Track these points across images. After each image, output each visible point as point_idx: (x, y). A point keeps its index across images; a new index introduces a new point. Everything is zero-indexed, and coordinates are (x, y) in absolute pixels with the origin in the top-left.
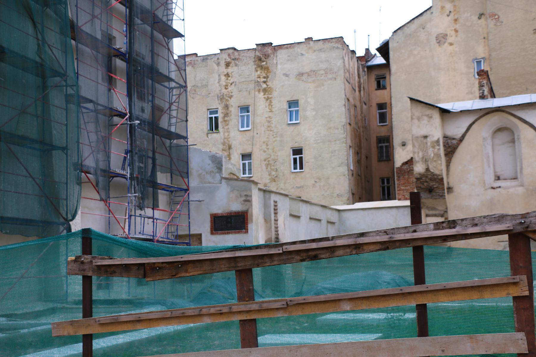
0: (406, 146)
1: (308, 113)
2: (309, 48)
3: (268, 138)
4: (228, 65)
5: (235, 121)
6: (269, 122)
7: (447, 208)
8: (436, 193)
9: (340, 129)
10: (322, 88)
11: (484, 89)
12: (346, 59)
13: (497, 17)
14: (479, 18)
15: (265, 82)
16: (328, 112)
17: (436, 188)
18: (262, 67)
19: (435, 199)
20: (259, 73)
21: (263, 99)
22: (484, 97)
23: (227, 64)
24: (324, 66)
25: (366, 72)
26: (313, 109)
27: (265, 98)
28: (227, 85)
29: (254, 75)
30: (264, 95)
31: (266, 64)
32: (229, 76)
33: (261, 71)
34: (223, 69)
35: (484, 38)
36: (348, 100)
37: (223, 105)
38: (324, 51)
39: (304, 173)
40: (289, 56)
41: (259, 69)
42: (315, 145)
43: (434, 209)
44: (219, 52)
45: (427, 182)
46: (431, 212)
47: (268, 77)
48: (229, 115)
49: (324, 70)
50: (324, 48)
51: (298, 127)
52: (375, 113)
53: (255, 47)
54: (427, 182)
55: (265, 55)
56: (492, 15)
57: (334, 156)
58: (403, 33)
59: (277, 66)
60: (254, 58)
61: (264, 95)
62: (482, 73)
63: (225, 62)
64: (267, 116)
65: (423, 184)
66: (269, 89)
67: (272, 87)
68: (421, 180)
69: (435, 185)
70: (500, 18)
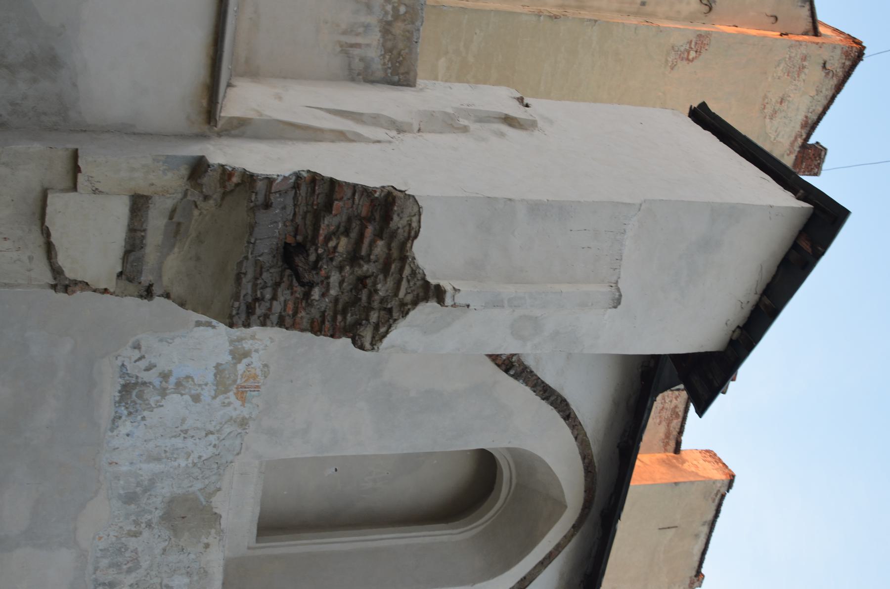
8: (277, 285)
13: (693, 54)
17: (307, 295)
45: (354, 258)
68: (370, 231)
69: (323, 295)
70: (685, 62)
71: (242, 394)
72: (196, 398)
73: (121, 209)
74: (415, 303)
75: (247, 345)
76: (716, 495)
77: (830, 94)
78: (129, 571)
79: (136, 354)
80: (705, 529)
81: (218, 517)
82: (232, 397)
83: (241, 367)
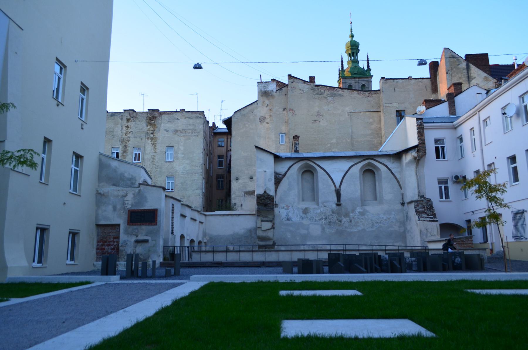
0: (238, 180)
1: (179, 155)
2: (183, 116)
3: (152, 169)
4: (128, 120)
5: (131, 156)
6: (153, 159)
7: (274, 217)
9: (199, 167)
10: (189, 140)
11: (297, 147)
12: (205, 125)
13: (293, 111)
14: (283, 111)
15: (152, 133)
16: (191, 156)
18: (151, 124)
19: (268, 210)
20: (149, 127)
21: (150, 144)
22: (297, 151)
23: (128, 119)
24: (191, 127)
25: (213, 136)
26: (183, 153)
27: (151, 143)
28: (127, 133)
29: (145, 129)
30: (151, 141)
31: (154, 122)
32: (129, 128)
33: (150, 126)
34: (125, 123)
35: (286, 122)
36: (204, 150)
37: (123, 145)
38: (192, 119)
39: (174, 192)
40: (169, 119)
41: (149, 125)
42: (182, 176)
43: (266, 217)
44: (123, 111)
45: (264, 199)
46: (265, 219)
47: (155, 131)
48: (127, 152)
49: (191, 130)
50: (191, 117)
51: (172, 163)
52: (217, 161)
53: (147, 111)
54: (264, 199)
55: (154, 117)
56: (291, 110)
57: (194, 183)
58: (241, 113)
59: (161, 124)
60: (147, 117)
61: (151, 141)
62: (296, 137)
63: (127, 118)
64: (152, 155)
65: (261, 201)
66: (155, 138)
67: (157, 137)
69: (269, 202)
71: (288, 207)
72: (289, 212)
73: (263, 223)
74: (267, 193)
75: (282, 207)
76: (386, 81)
77: (298, 80)
78: (313, 217)
79: (284, 219)
80: (395, 81)
81: (306, 208)
82: (289, 208)
83: (285, 207)
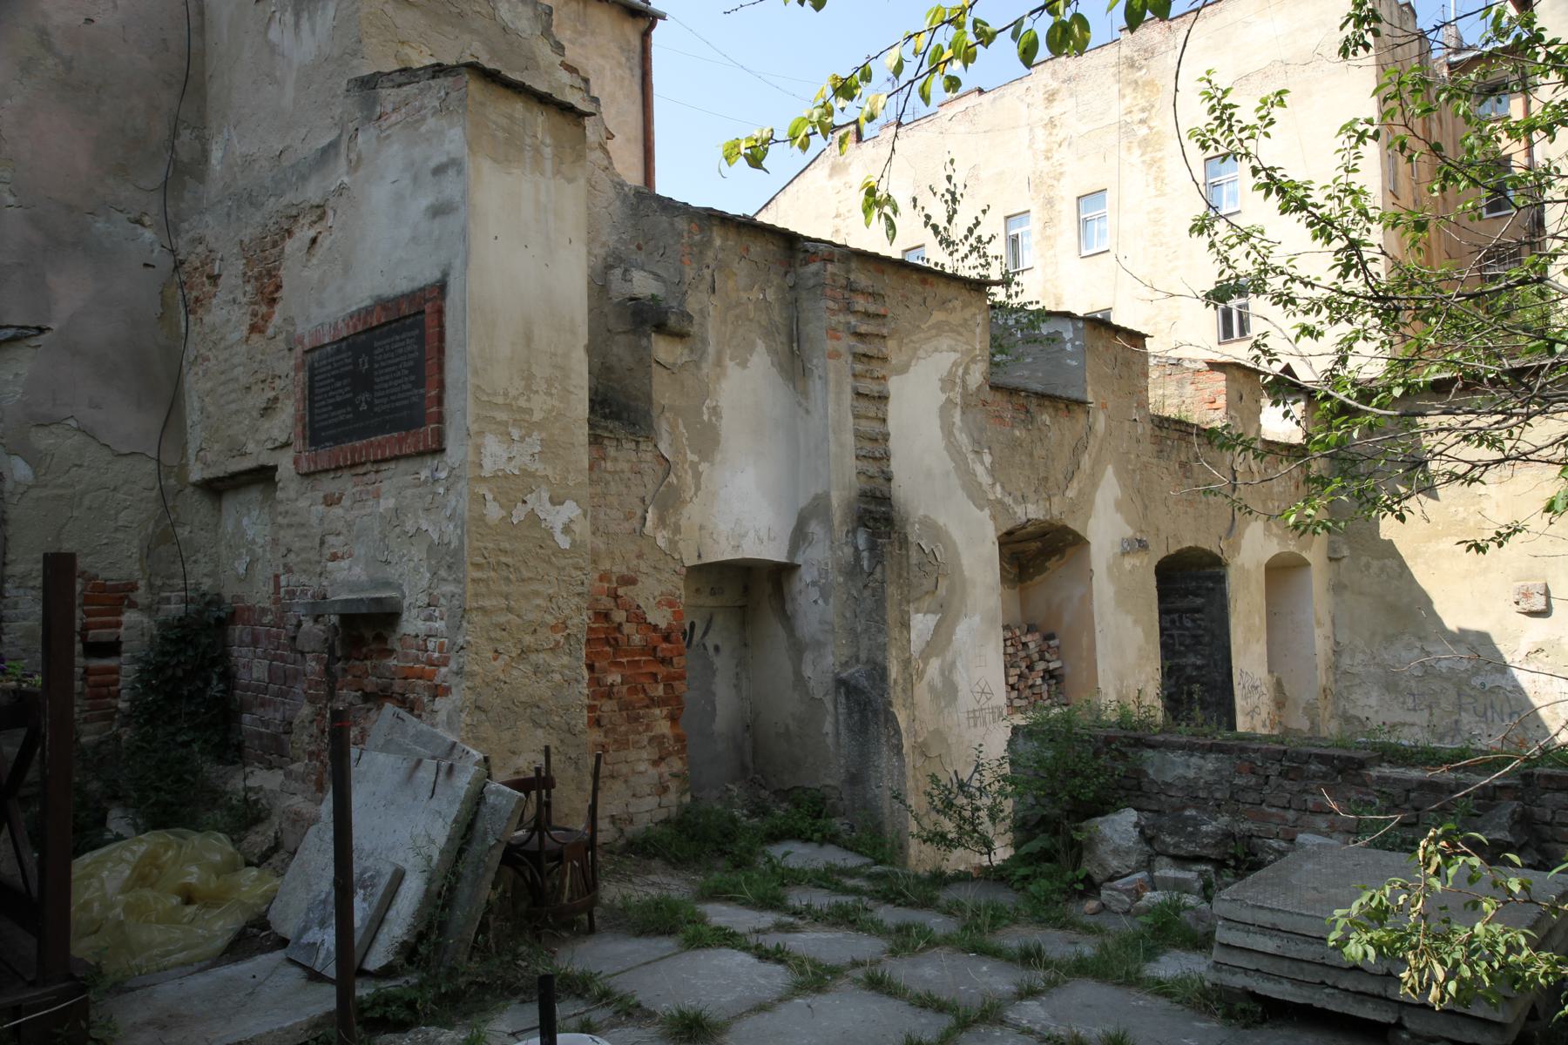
15: (1142, 121)
20: (1128, 101)
27: (1144, 162)
28: (1050, 150)
34: (1040, 113)
